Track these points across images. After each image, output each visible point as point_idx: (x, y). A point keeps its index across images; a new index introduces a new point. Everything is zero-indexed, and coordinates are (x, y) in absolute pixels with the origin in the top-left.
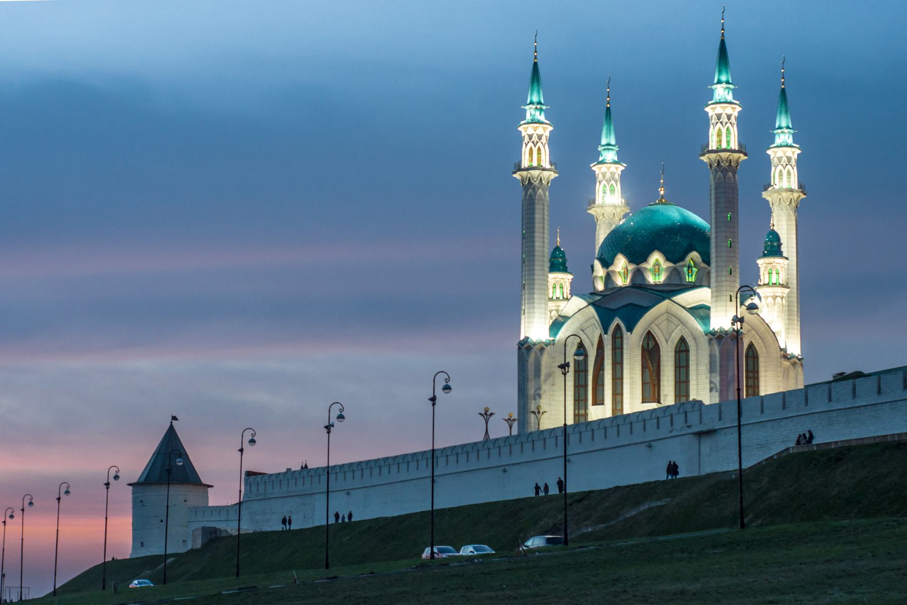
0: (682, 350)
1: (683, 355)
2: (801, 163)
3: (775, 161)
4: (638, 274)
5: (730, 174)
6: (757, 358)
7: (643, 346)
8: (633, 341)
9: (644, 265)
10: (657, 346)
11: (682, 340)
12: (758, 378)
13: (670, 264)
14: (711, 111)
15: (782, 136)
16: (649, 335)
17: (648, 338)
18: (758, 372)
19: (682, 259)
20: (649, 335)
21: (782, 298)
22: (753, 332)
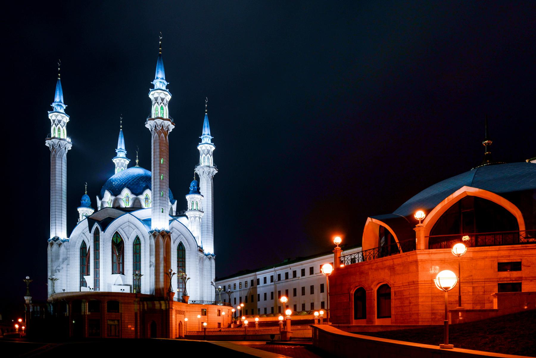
0: (137, 243)
1: (138, 246)
2: (215, 154)
3: (201, 152)
4: (116, 201)
5: (163, 134)
6: (185, 251)
7: (113, 241)
8: (106, 237)
9: (119, 196)
10: (122, 242)
11: (137, 238)
12: (185, 262)
13: (134, 196)
14: (152, 95)
15: (205, 139)
16: (117, 234)
17: (117, 236)
18: (185, 259)
19: (141, 193)
20: (117, 234)
21: (200, 218)
22: (182, 236)
